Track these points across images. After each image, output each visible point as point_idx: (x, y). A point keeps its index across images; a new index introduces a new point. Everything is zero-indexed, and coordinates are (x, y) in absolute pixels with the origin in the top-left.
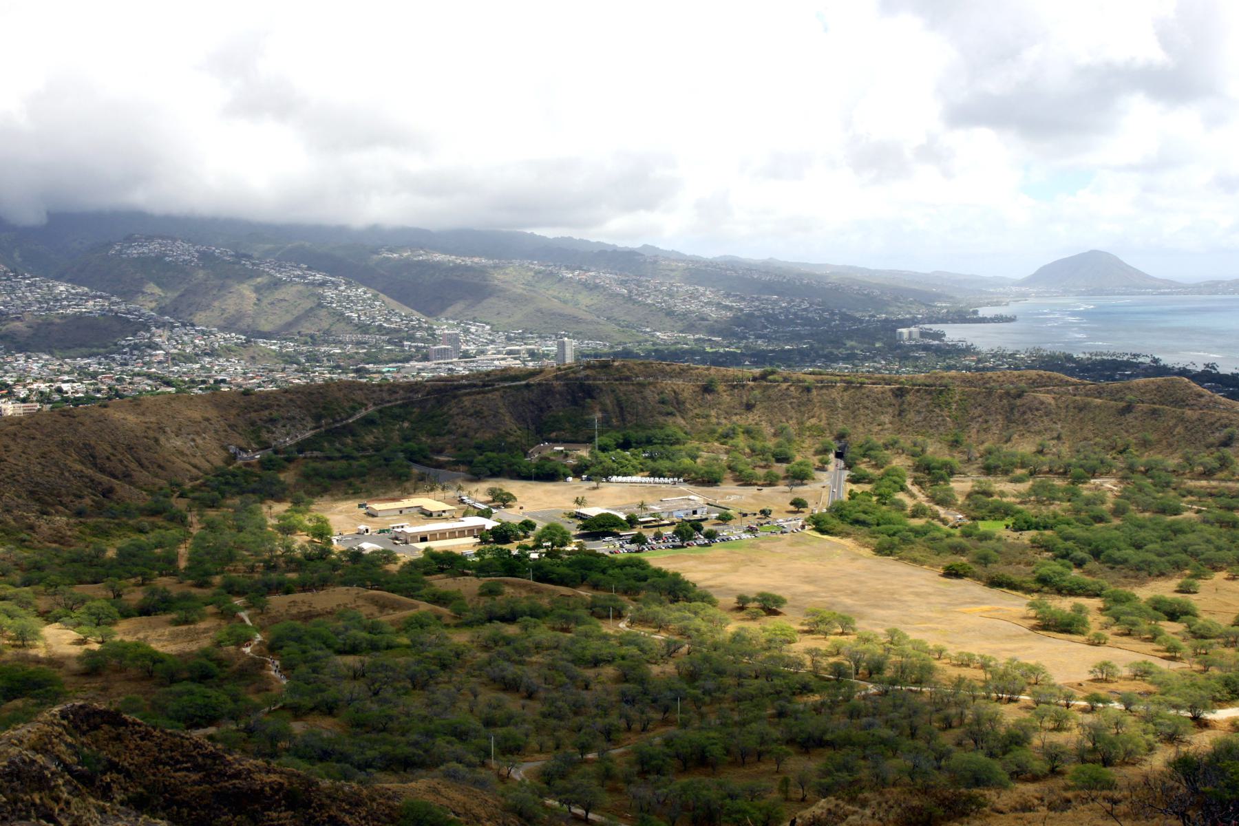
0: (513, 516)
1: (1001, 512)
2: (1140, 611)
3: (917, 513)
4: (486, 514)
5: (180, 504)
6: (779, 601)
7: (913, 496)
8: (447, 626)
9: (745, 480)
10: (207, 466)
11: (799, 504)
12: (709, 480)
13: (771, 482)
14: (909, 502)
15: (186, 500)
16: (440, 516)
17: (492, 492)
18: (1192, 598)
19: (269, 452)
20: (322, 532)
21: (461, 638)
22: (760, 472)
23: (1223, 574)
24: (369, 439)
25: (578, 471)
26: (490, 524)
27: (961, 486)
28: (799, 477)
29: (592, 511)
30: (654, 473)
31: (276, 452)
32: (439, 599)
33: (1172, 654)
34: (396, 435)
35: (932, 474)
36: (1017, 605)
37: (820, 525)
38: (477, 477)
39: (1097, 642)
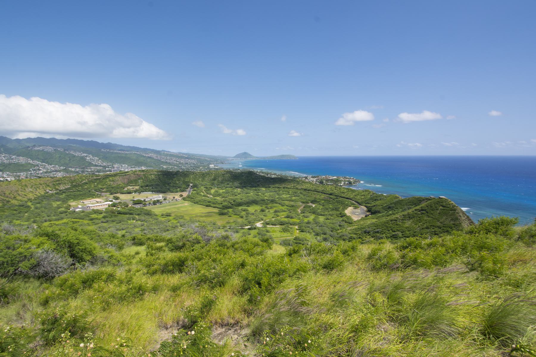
0: (118, 201)
1: (219, 195)
3: (204, 196)
4: (112, 201)
5: (29, 204)
10: (39, 195)
11: (181, 196)
14: (202, 194)
16: (100, 202)
24: (86, 187)
25: (135, 192)
26: (111, 203)
27: (213, 191)
28: (183, 191)
29: (135, 199)
30: (153, 191)
31: (60, 191)
34: (93, 186)
35: (208, 189)
37: (184, 199)
38: (111, 194)
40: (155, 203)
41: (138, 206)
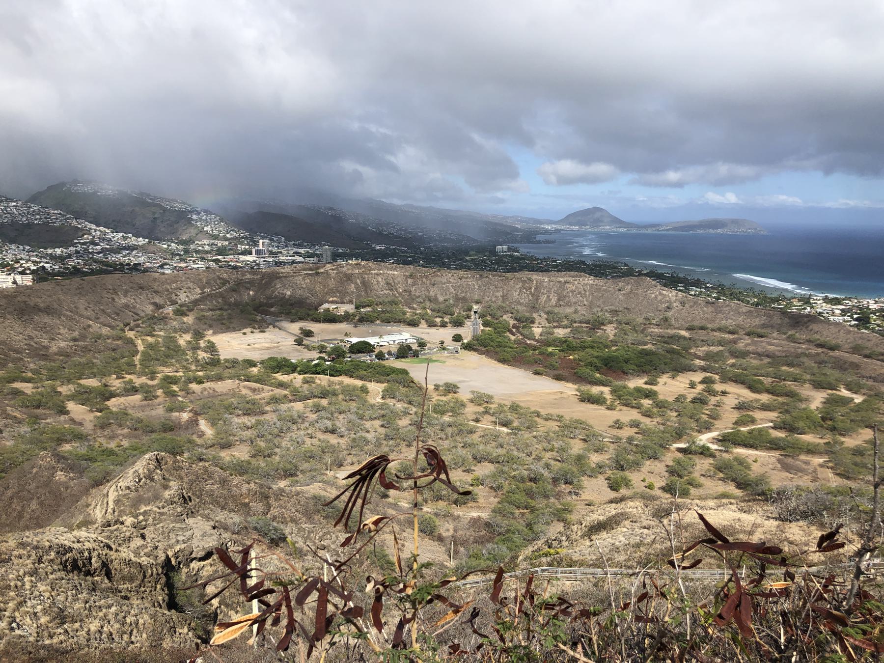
2: (631, 394)
6: (455, 386)
7: (513, 334)
8: (290, 401)
9: (432, 325)
12: (413, 324)
13: (444, 325)
15: (133, 332)
17: (301, 329)
18: (654, 388)
19: (177, 306)
20: (212, 348)
21: (298, 406)
22: (438, 320)
23: (668, 375)
25: (346, 318)
32: (281, 385)
33: (647, 414)
36: (570, 389)
39: (610, 408)
40: (404, 351)
41: (366, 358)
